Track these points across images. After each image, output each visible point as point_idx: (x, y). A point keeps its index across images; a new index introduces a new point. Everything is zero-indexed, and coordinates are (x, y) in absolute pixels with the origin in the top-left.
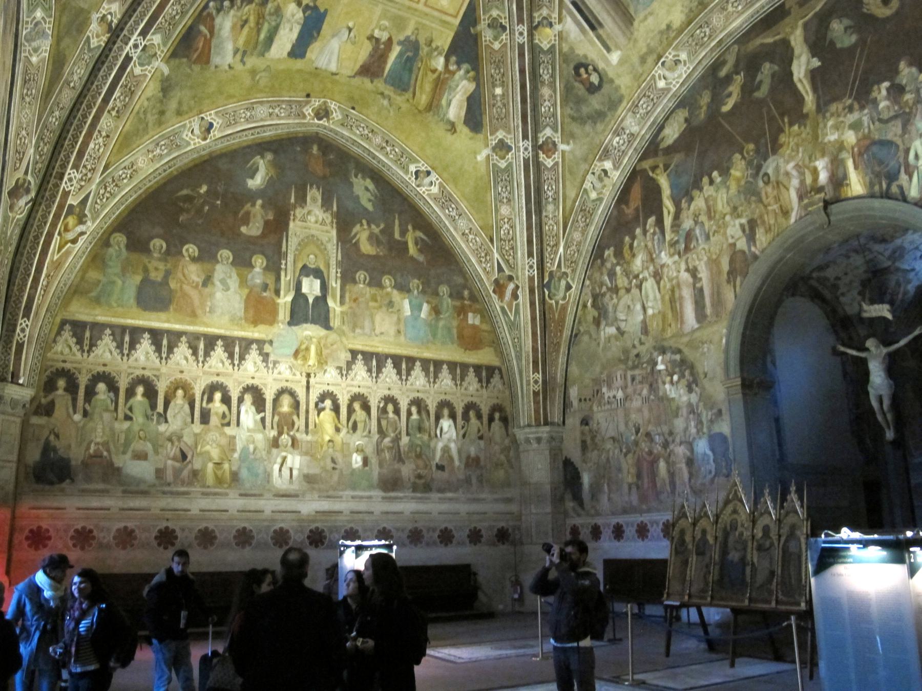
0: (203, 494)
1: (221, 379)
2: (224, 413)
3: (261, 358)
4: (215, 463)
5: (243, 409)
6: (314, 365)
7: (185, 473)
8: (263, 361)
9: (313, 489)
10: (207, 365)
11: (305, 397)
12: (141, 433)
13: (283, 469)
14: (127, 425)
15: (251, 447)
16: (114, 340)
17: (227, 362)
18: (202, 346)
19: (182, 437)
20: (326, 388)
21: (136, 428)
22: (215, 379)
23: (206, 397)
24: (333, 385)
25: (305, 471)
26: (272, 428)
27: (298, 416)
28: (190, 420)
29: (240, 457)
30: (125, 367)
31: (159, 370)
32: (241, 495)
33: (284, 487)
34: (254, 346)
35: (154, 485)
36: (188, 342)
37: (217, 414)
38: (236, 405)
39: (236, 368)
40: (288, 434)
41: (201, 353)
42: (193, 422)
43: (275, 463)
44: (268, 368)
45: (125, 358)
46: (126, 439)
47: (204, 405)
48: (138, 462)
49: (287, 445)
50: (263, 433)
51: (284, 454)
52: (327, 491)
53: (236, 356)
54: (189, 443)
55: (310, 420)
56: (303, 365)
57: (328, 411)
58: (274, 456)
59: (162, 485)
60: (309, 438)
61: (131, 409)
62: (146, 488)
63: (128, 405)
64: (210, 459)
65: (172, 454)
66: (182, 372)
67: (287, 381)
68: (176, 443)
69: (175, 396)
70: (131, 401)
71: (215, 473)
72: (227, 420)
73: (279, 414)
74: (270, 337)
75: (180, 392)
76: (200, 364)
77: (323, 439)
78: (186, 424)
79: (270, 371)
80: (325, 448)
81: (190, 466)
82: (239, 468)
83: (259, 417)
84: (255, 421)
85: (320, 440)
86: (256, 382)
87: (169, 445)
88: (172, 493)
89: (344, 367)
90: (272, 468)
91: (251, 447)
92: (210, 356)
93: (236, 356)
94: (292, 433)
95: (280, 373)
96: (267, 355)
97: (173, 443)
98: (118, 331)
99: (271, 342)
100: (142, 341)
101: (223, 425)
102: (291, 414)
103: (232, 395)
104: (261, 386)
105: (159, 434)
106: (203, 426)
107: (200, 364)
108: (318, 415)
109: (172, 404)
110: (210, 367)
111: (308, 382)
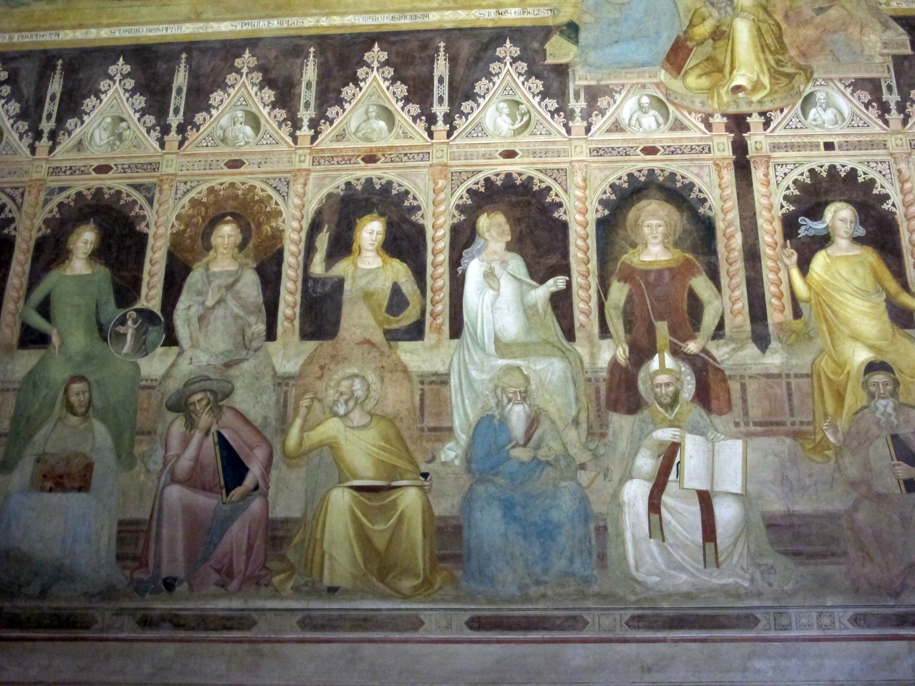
0: (309, 622)
1: (380, 173)
2: (396, 290)
3: (537, 85)
4: (358, 489)
5: (474, 270)
6: (757, 86)
7: (237, 532)
8: (544, 95)
9: (824, 585)
10: (327, 131)
11: (732, 203)
12: (76, 387)
13: (665, 498)
14: (28, 359)
15: (517, 415)
16: (16, 95)
17: (404, 115)
18: (310, 72)
19: (228, 394)
20: (822, 161)
21: (59, 372)
22: (360, 173)
23: (323, 241)
24: (847, 146)
25: (776, 506)
26: (604, 331)
27: (714, 275)
28: (261, 327)
29: (468, 459)
30: (40, 171)
31: (154, 167)
32: (477, 623)
33: (682, 581)
34: (508, 50)
35: (109, 593)
36: (261, 68)
37: (367, 296)
38: (444, 257)
39: (440, 127)
40: (676, 352)
41: (307, 95)
42: (271, 335)
43: (627, 475)
44: (570, 115)
45: (45, 143)
46: (15, 420)
47: (318, 267)
48: (57, 498)
49: (675, 398)
50: (564, 354)
51: (666, 434)
52: (897, 595)
53: (441, 90)
54: (255, 413)
55: (770, 289)
56: (711, 90)
57: (842, 245)
58: (623, 445)
59: (140, 589)
60: (774, 360)
61: (45, 309)
62: (79, 604)
63: (38, 295)
64: (342, 473)
65: (185, 463)
66: (235, 164)
67: (650, 151)
68: (205, 419)
69: (208, 247)
70: (50, 280)
71: (364, 538)
72: (409, 317)
73: (628, 276)
74: (563, 19)
75: (227, 233)
76: (305, 132)
77: (840, 365)
78: (243, 342)
79: (578, 124)
80: (854, 398)
81: (256, 505)
82: (468, 500)
83: (541, 293)
84: (528, 311)
85: (825, 365)
86: (518, 167)
87: (178, 426)
88: (177, 622)
89: (888, 77)
90: (616, 497)
91: (517, 415)
92: (340, 102)
93: (441, 90)
94: (692, 347)
95: (617, 127)
96: (562, 71)
97: (191, 424)
98: (28, 71)
99: (572, 30)
100: (103, 85)
101: (393, 336)
102: (681, 272)
103: (428, 224)
104: (542, 180)
105: (135, 380)
106: (311, 345)
107: (305, 132)
108: (804, 265)
109: (195, 277)
110: (341, 137)
111: (740, 148)
